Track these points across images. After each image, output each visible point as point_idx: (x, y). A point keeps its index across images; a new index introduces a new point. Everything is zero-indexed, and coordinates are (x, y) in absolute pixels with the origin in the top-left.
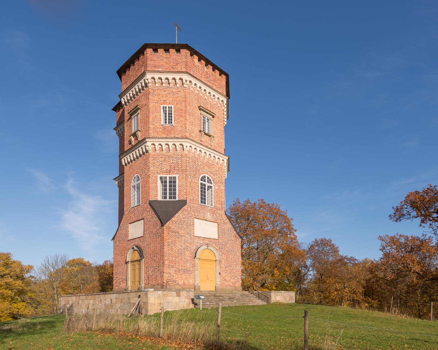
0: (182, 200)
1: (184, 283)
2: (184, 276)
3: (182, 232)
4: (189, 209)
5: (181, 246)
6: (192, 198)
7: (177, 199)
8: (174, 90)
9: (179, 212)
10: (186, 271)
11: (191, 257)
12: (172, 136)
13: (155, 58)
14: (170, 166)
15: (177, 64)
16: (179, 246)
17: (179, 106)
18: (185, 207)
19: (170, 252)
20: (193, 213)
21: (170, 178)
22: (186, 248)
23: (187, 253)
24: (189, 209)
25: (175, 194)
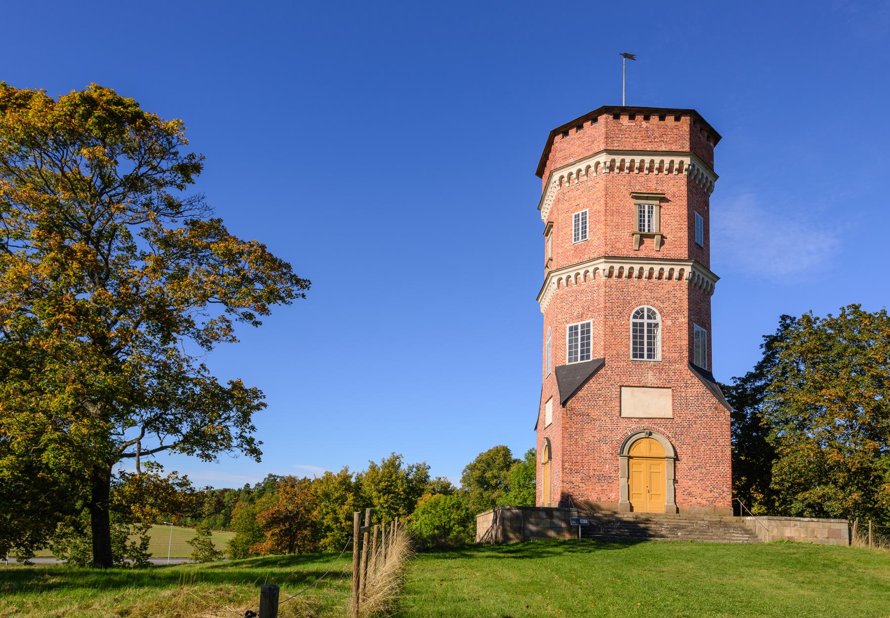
0: (598, 360)
1: (599, 499)
2: (598, 488)
3: (594, 413)
4: (609, 372)
5: (594, 437)
6: (615, 353)
7: (591, 359)
8: (590, 184)
9: (591, 381)
10: (602, 478)
11: (612, 454)
12: (586, 257)
13: (565, 145)
14: (583, 307)
15: (593, 142)
16: (588, 436)
17: (596, 207)
18: (602, 371)
19: (573, 447)
20: (618, 379)
21: (582, 326)
22: (603, 440)
23: (605, 448)
24: (609, 372)
25: (588, 350)
